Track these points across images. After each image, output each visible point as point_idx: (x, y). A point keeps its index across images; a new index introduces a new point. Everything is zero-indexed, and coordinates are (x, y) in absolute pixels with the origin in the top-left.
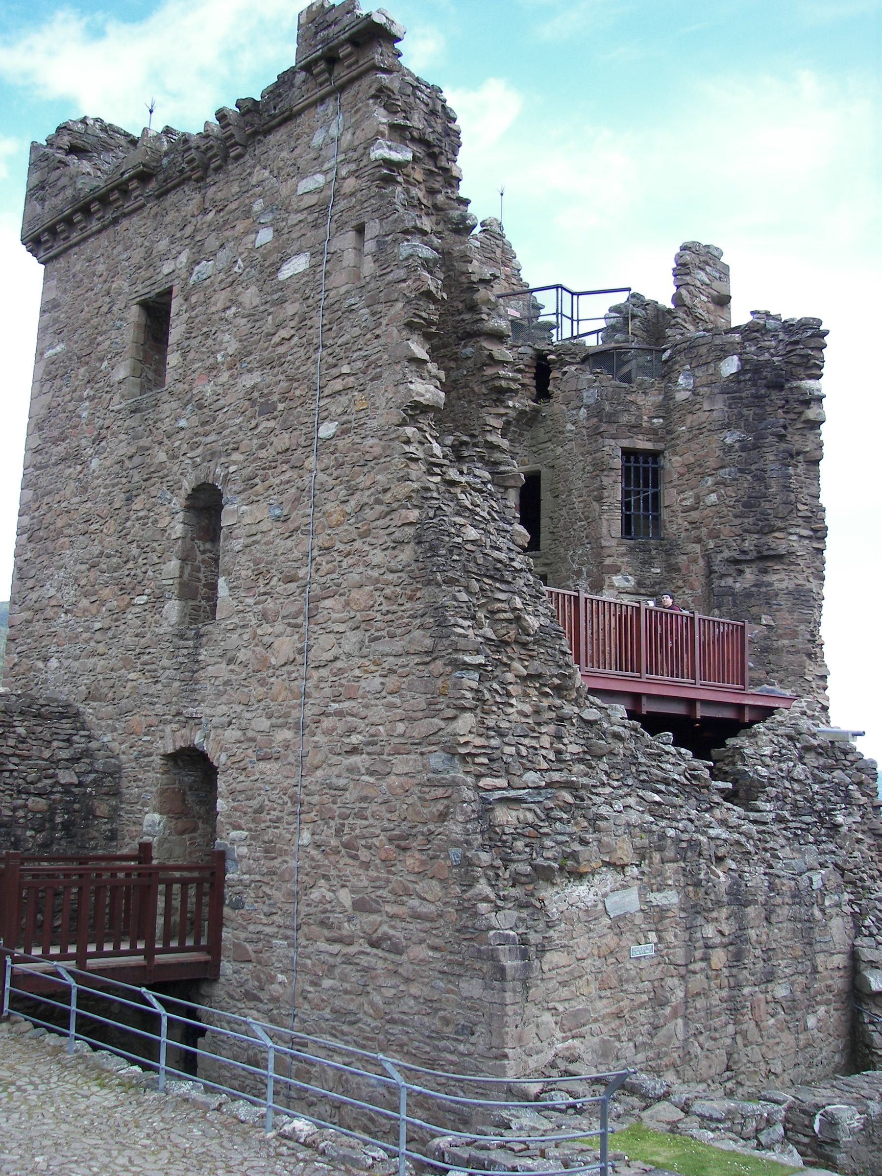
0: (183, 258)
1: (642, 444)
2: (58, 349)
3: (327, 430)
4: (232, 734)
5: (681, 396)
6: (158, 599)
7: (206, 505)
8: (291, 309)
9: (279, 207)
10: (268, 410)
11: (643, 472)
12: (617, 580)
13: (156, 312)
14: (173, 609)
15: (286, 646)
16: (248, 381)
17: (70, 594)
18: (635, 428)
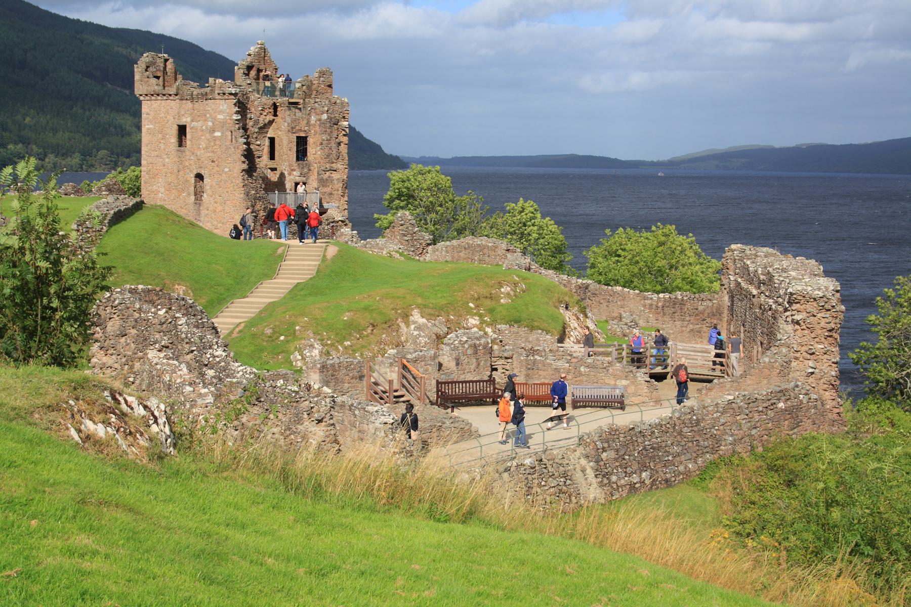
0: (189, 119)
1: (303, 135)
2: (151, 126)
3: (227, 170)
4: (209, 224)
5: (313, 122)
6: (189, 194)
7: (200, 177)
8: (217, 143)
9: (214, 119)
10: (213, 161)
11: (302, 143)
12: (295, 173)
13: (182, 130)
14: (193, 198)
15: (220, 208)
16: (209, 154)
17: (162, 190)
18: (301, 130)
